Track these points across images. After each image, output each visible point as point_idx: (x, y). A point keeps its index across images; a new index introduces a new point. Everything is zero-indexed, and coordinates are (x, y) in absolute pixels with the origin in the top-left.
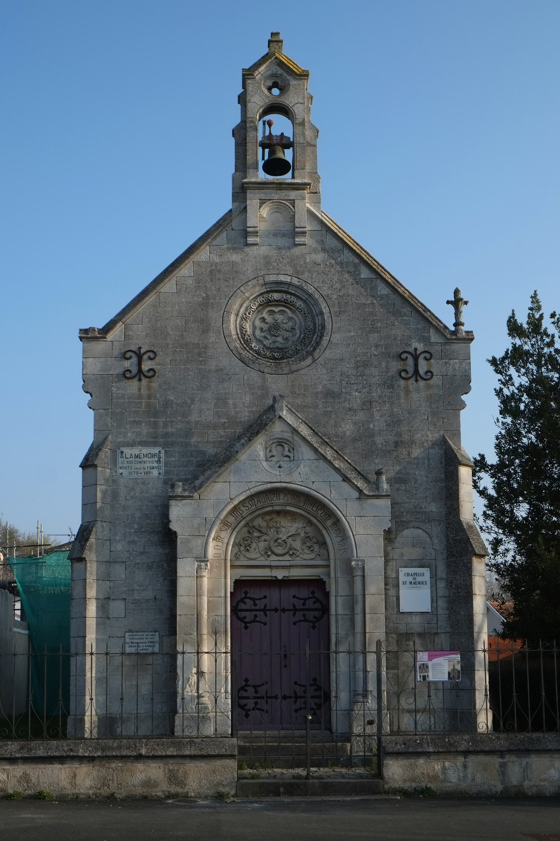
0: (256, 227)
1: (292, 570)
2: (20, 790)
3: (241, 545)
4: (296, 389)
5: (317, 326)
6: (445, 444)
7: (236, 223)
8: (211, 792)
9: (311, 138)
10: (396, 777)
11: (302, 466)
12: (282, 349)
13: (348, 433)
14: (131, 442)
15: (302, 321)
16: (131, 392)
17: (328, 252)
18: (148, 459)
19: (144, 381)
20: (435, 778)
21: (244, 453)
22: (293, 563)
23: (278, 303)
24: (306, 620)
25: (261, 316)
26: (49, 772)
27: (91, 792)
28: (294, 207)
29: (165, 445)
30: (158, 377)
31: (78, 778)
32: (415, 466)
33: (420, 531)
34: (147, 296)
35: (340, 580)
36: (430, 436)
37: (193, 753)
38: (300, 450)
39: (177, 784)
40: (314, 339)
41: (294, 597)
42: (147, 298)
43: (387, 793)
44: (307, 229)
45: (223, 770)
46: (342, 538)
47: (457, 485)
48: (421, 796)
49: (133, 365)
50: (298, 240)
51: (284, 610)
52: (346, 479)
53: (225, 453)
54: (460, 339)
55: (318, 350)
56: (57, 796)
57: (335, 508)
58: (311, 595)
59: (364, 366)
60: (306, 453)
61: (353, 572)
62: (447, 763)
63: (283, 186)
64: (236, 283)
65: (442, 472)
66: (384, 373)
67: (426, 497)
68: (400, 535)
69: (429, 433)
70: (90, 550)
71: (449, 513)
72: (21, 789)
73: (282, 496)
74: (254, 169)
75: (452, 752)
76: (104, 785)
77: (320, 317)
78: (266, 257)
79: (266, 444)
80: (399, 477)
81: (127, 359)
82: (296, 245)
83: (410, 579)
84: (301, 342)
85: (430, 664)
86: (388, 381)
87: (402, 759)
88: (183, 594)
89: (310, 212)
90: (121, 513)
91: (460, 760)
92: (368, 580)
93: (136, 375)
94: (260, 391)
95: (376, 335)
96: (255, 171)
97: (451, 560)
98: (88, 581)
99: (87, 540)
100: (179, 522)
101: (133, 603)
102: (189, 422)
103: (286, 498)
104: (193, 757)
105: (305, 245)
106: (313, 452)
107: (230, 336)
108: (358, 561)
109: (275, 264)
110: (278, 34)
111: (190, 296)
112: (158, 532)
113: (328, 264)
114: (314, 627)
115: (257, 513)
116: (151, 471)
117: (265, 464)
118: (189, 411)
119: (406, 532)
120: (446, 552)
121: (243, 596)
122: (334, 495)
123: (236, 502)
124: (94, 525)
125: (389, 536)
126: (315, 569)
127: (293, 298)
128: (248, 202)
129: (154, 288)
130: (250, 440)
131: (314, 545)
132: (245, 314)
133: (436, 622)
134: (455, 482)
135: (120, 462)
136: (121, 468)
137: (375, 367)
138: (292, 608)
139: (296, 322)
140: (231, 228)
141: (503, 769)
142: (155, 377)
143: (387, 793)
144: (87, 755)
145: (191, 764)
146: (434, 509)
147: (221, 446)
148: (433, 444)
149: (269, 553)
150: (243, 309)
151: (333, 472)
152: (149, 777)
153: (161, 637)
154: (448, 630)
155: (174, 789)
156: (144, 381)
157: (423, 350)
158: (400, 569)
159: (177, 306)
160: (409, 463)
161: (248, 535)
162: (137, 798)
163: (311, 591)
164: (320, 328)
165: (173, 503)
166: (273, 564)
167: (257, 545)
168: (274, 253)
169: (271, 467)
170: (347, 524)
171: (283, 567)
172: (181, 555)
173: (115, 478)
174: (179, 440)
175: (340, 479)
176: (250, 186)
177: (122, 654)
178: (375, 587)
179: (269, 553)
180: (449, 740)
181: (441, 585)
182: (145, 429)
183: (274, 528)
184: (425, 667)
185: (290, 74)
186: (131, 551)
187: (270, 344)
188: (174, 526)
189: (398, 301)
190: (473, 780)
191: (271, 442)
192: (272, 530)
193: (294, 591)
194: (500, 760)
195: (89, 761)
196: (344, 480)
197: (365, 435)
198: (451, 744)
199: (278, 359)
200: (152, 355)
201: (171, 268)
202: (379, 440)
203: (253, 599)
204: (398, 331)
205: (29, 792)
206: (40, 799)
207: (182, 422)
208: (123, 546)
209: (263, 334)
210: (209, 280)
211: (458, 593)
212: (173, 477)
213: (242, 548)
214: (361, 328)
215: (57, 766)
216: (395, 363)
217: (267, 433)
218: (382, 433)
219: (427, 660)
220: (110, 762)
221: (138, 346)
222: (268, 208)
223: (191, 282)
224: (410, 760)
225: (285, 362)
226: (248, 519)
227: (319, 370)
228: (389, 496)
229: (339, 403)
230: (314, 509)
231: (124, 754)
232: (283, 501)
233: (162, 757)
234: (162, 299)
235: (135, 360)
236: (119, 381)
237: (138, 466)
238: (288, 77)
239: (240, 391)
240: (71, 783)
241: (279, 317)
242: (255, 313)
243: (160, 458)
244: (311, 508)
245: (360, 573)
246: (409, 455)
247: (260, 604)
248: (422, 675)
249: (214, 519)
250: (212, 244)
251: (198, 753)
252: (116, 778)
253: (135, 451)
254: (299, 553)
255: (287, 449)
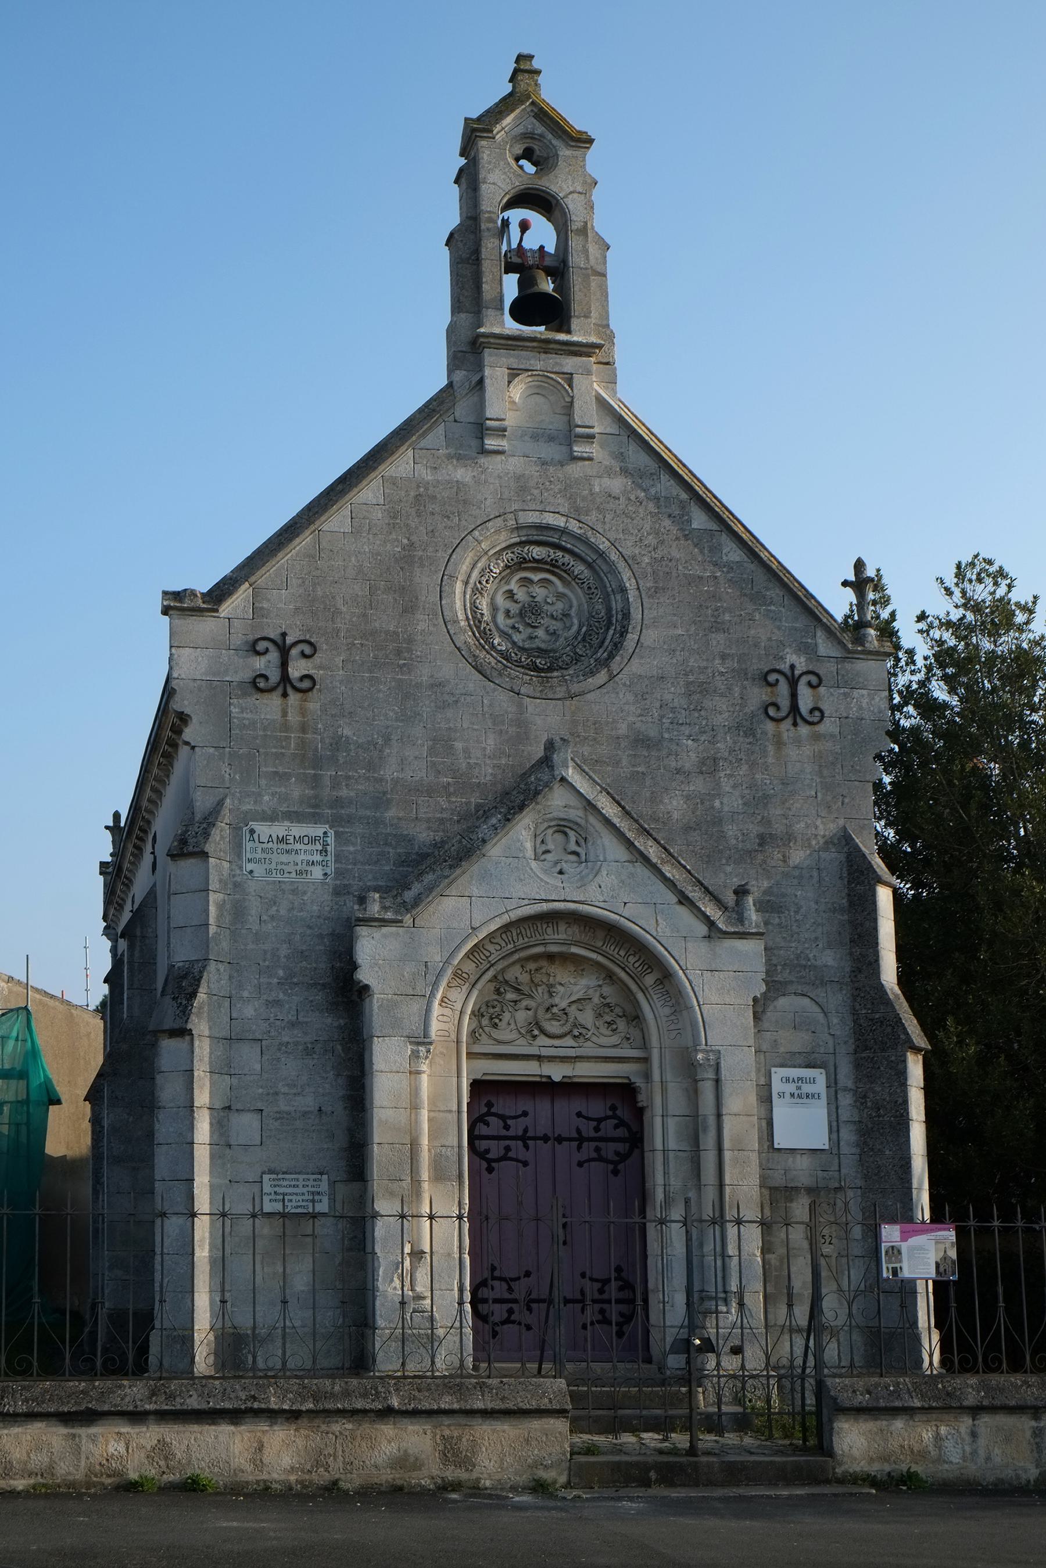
0: (503, 420)
1: (579, 1065)
2: (152, 1472)
3: (483, 1016)
4: (580, 728)
5: (614, 612)
6: (847, 844)
7: (462, 410)
8: (523, 1479)
9: (597, 259)
10: (855, 1452)
11: (604, 873)
12: (546, 651)
13: (676, 815)
14: (269, 812)
15: (584, 600)
16: (268, 717)
17: (632, 475)
18: (303, 847)
19: (294, 698)
20: (922, 1455)
21: (496, 844)
22: (579, 1052)
23: (538, 565)
24: (601, 1159)
25: (507, 588)
26: (210, 1440)
27: (293, 1478)
28: (571, 386)
29: (335, 822)
30: (320, 690)
31: (266, 1451)
32: (795, 882)
33: (807, 1001)
34: (298, 536)
35: (671, 1086)
36: (821, 827)
37: (490, 1406)
38: (599, 842)
39: (458, 1465)
40: (609, 637)
41: (579, 1115)
42: (297, 540)
43: (841, 1481)
44: (596, 430)
45: (544, 1439)
46: (673, 1009)
47: (875, 920)
48: (904, 1488)
49: (271, 665)
50: (578, 449)
51: (560, 1140)
52: (684, 900)
53: (460, 842)
54: (870, 653)
55: (618, 658)
56: (226, 1486)
57: (666, 953)
58: (610, 1113)
59: (701, 692)
60: (610, 848)
61: (696, 1072)
62: (942, 1428)
63: (552, 346)
64: (463, 523)
65: (844, 895)
66: (737, 708)
67: (816, 938)
68: (771, 1008)
69: (819, 822)
70: (199, 1015)
71: (856, 971)
72: (153, 1471)
73: (562, 927)
74: (497, 309)
75: (951, 1408)
76: (318, 1464)
77: (619, 597)
78: (518, 478)
79: (536, 829)
80: (769, 901)
81: (258, 653)
82: (575, 459)
83: (791, 1088)
84: (584, 640)
85: (904, 1247)
86: (744, 723)
87: (866, 1420)
88: (385, 1103)
89: (601, 401)
90: (250, 946)
91: (966, 1423)
92: (727, 1089)
93: (278, 684)
94: (514, 729)
95: (721, 637)
96: (498, 313)
97: (863, 1055)
98: (196, 1074)
99: (193, 995)
100: (376, 969)
101: (276, 1119)
102: (381, 780)
103: (570, 931)
104: (487, 1414)
105: (590, 459)
106: (623, 848)
107: (456, 621)
108: (707, 1051)
109: (536, 492)
110: (530, 57)
111: (378, 542)
112: (323, 985)
113: (633, 497)
114: (616, 1172)
115: (516, 956)
116: (309, 868)
117: (534, 864)
118: (381, 758)
119: (782, 1002)
120: (852, 1040)
121: (485, 1110)
122: (663, 929)
123: (482, 935)
124: (204, 967)
125: (760, 1008)
126: (620, 1065)
127: (567, 558)
128: (487, 372)
129: (310, 522)
130: (509, 820)
131: (618, 1020)
132: (480, 582)
133: (837, 1168)
134: (869, 914)
135: (248, 849)
136: (250, 861)
137: (722, 695)
138: (576, 1136)
139: (570, 600)
140: (454, 416)
141: (1037, 1440)
142: (315, 690)
143: (841, 1481)
144: (286, 1407)
145: (484, 1427)
146: (831, 962)
147: (442, 827)
148: (826, 843)
149: (536, 1032)
150: (475, 574)
151: (661, 887)
152: (406, 1451)
153: (332, 1184)
154: (859, 1183)
155: (452, 1474)
156: (294, 698)
157: (805, 669)
158: (773, 1070)
159: (353, 559)
160: (786, 875)
161: (496, 997)
162: (383, 1489)
163: (609, 1104)
164: (620, 617)
165: (362, 931)
166: (545, 1052)
167: (513, 1017)
168: (533, 471)
169: (545, 871)
170: (687, 984)
171: (564, 1059)
172: (381, 1031)
173: (238, 879)
174: (362, 812)
175: (674, 899)
176: (492, 340)
177: (254, 1216)
178: (739, 1103)
179: (536, 1032)
180: (944, 1387)
181: (846, 1100)
182: (296, 791)
183: (544, 986)
184: (895, 1252)
185: (559, 137)
186: (272, 1020)
187: (523, 641)
188: (364, 976)
189: (760, 575)
190: (988, 1459)
191: (546, 825)
192: (540, 989)
193: (578, 1104)
194: (1033, 1423)
195: (287, 1419)
196: (680, 903)
197: (707, 824)
198: (948, 1394)
199: (542, 670)
200: (308, 650)
201: (340, 487)
202: (731, 831)
203: (503, 1118)
204: (763, 631)
205: (171, 1478)
206: (194, 1490)
207: (368, 778)
208: (255, 1010)
209: (510, 622)
210: (414, 513)
211: (879, 1116)
212: (351, 882)
213: (485, 1022)
214: (695, 623)
215: (225, 1429)
216: (756, 690)
217: (539, 807)
218: (736, 817)
219: (899, 1239)
220: (329, 1422)
221: (279, 631)
222: (523, 386)
223: (380, 515)
224: (879, 1423)
225: (557, 677)
226: (500, 966)
227: (621, 696)
228: (762, 934)
229: (658, 759)
230: (622, 953)
231: (359, 1406)
232: (564, 936)
233: (430, 1413)
234: (324, 544)
235: (274, 656)
236: (245, 694)
237: (284, 858)
238: (555, 142)
239: (476, 727)
240: (253, 1461)
241: (540, 592)
242: (497, 580)
243: (325, 845)
244: (617, 950)
245: (711, 1075)
246: (784, 861)
247: (517, 1127)
248: (891, 1266)
249: (441, 964)
250: (418, 446)
251: (498, 1405)
252: (340, 1453)
253: (279, 829)
254: (590, 1034)
255: (573, 839)
